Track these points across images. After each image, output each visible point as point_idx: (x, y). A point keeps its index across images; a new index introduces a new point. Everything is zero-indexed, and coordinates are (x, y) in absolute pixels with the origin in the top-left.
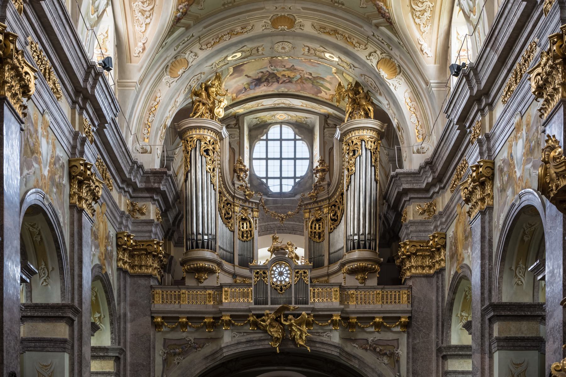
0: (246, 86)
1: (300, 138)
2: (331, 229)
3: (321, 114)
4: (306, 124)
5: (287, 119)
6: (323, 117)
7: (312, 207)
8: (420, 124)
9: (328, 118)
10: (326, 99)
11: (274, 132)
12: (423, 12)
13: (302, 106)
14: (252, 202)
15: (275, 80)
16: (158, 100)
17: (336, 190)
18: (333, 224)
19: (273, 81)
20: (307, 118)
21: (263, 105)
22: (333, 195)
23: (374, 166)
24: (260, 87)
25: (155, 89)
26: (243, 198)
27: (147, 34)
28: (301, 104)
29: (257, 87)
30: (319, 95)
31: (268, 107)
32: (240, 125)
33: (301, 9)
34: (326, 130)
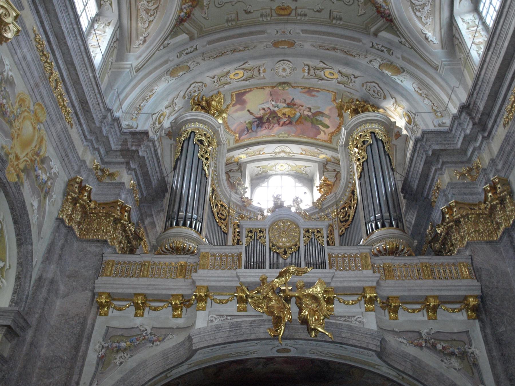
0: (249, 126)
4: (305, 173)
5: (287, 170)
6: (322, 164)
8: (435, 105)
10: (325, 141)
12: (423, 6)
14: (251, 211)
15: (276, 121)
16: (154, 91)
17: (345, 191)
20: (306, 167)
24: (262, 129)
27: (149, 30)
28: (300, 151)
29: (259, 129)
30: (318, 137)
31: (268, 156)
32: (242, 170)
33: (301, 33)
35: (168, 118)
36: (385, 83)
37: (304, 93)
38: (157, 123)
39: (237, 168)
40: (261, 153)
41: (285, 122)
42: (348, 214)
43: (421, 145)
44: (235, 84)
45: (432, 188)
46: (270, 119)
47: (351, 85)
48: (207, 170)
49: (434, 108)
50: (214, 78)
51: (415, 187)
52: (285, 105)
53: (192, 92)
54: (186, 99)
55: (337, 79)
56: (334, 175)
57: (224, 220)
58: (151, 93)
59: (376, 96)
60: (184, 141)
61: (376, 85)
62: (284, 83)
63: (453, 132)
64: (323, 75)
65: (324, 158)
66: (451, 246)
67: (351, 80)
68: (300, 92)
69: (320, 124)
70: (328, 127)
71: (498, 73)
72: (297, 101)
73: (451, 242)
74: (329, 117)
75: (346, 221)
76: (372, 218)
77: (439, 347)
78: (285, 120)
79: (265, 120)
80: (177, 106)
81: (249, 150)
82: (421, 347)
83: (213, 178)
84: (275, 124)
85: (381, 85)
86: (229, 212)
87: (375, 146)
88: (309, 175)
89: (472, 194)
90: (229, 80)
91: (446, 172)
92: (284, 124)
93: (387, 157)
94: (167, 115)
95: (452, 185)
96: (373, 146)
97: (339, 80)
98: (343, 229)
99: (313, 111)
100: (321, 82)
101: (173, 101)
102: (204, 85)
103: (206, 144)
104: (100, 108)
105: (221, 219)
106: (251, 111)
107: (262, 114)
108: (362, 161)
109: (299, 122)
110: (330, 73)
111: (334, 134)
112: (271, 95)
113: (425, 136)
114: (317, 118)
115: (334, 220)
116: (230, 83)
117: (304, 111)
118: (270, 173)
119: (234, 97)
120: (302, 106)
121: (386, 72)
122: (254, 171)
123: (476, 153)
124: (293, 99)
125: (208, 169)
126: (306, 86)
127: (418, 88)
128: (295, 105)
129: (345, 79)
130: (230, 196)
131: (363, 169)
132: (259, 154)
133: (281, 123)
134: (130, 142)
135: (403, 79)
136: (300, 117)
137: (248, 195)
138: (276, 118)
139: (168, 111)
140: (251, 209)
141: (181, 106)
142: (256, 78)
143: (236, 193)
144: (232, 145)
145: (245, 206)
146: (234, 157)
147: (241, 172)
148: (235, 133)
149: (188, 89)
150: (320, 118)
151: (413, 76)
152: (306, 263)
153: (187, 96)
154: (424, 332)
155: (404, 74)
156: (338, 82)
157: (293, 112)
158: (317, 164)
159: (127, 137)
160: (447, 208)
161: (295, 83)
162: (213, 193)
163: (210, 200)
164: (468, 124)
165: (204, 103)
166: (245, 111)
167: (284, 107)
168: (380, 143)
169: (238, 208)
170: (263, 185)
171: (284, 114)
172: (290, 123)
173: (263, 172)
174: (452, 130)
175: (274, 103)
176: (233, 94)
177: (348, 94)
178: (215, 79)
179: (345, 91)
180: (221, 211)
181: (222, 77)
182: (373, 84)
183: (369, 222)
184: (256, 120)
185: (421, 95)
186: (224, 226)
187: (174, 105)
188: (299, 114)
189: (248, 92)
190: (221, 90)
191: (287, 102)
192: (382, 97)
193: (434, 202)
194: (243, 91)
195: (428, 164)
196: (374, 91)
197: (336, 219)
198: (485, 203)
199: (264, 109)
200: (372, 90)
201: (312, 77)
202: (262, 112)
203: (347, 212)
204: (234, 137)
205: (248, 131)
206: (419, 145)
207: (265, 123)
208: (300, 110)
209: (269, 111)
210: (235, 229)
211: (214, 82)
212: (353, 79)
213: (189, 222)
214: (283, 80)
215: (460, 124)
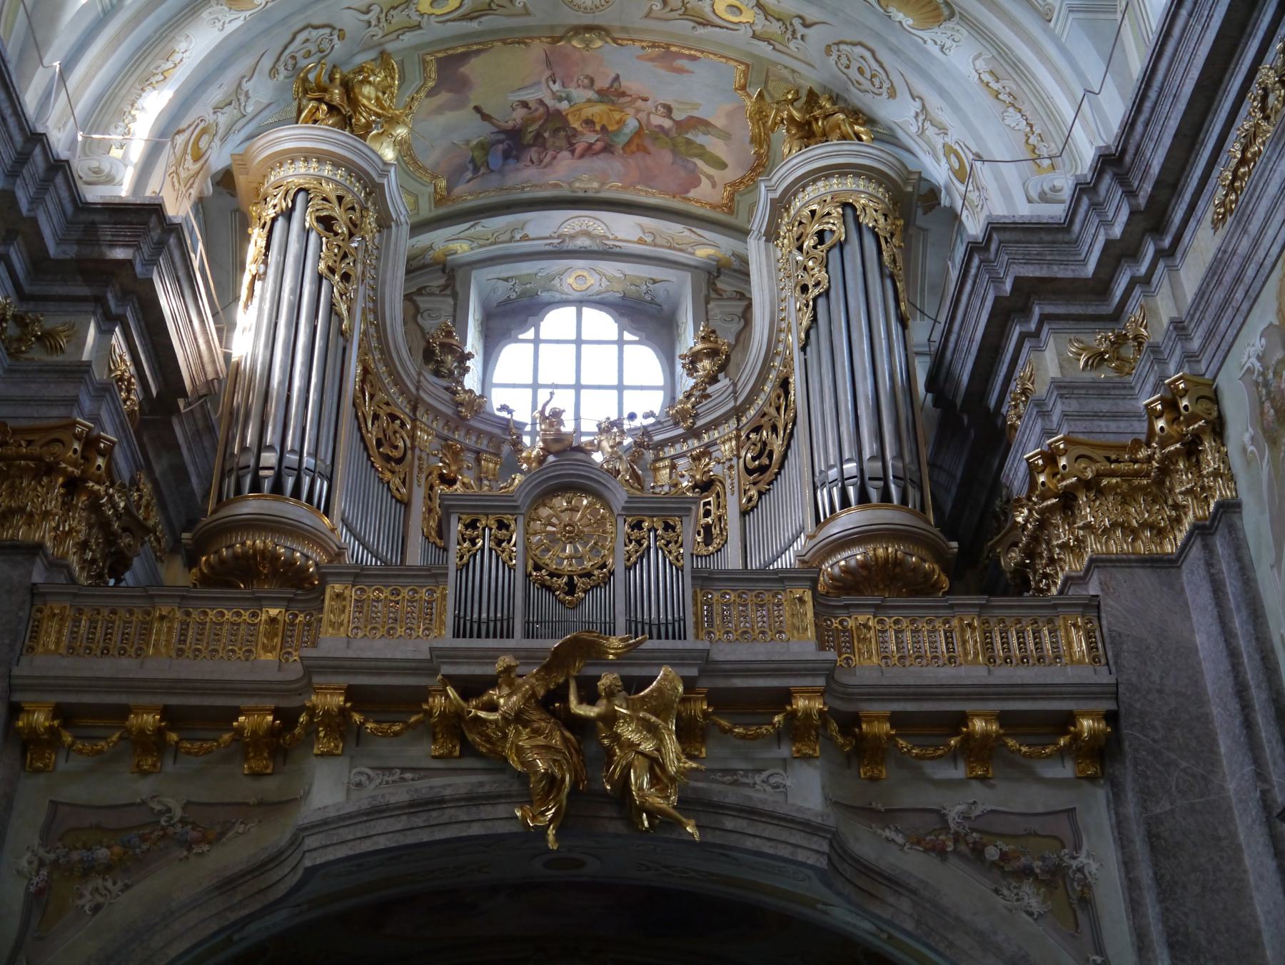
0: (477, 154)
1: (637, 338)
2: (750, 500)
3: (696, 267)
5: (596, 288)
6: (704, 276)
7: (678, 451)
8: (1037, 130)
9: (718, 277)
10: (713, 207)
11: (558, 322)
13: (641, 241)
14: (480, 433)
15: (564, 143)
16: (177, 58)
17: (762, 378)
18: (755, 484)
19: (558, 144)
20: (655, 282)
21: (525, 238)
22: (750, 400)
23: (892, 277)
24: (521, 165)
25: (172, 35)
26: (449, 412)
30: (692, 194)
31: (539, 245)
32: (458, 288)
34: (711, 305)
35: (223, 140)
36: (895, 51)
37: (652, 60)
38: (189, 157)
39: (442, 282)
40: (518, 237)
41: (590, 146)
42: (768, 448)
43: (981, 261)
44: (434, 31)
45: (1012, 387)
46: (546, 135)
47: (792, 45)
48: (345, 313)
49: (1033, 140)
50: (367, 12)
51: (965, 379)
52: (591, 94)
53: (299, 55)
54: (281, 77)
55: (751, 25)
56: (739, 311)
57: (399, 461)
58: (170, 65)
59: (866, 84)
60: (274, 220)
61: (868, 55)
62: (589, 28)
63: (1076, 227)
64: (708, 9)
65: (709, 257)
66: (1047, 565)
67: (794, 32)
68: (639, 58)
69: (700, 156)
70: (723, 166)
71: (1201, 74)
72: (626, 84)
73: (1050, 551)
74: (726, 136)
75: (762, 469)
76: (833, 473)
77: (992, 853)
78: (592, 138)
79: (529, 138)
80: (251, 102)
81: (479, 228)
82: (942, 853)
83: (365, 333)
84: (561, 149)
85: (884, 55)
86: (413, 437)
87: (852, 250)
88: (665, 307)
89: (1115, 416)
90: (416, 18)
91: (1051, 342)
92: (589, 150)
93: (888, 283)
94: (221, 131)
95: (1063, 388)
96: (847, 249)
97: (758, 28)
98: (753, 492)
99: (678, 116)
100: (701, 31)
101: (239, 85)
102: (336, 33)
103: (342, 229)
104: (8, 131)
105: (388, 458)
106: (486, 111)
107: (519, 121)
108: (813, 292)
109: (634, 147)
110: (731, 6)
111: (742, 187)
112: (549, 63)
113: (995, 236)
114: (689, 136)
115: (728, 464)
116: (419, 27)
117: (649, 114)
118: (545, 296)
119: (433, 68)
120: (645, 100)
121: (900, 16)
122: (494, 290)
123: (1137, 291)
124: (617, 78)
125: (349, 310)
126: (656, 39)
127: (991, 73)
128: (623, 94)
129: (775, 27)
130: (417, 389)
131: (815, 319)
132: (511, 239)
133: (580, 148)
134: (106, 232)
135: (949, 43)
136: (639, 132)
137: (471, 381)
138: (562, 134)
139: (223, 119)
140: (482, 426)
141: (265, 101)
142: (501, 11)
143: (437, 373)
144: (427, 210)
145: (464, 419)
146: (431, 248)
147: (455, 296)
148: (436, 177)
149: (286, 48)
150: (700, 139)
151: (979, 31)
152: (629, 621)
153: (282, 69)
154: (953, 813)
155: (950, 24)
156: (754, 36)
157: (617, 116)
158: (688, 277)
159: (97, 218)
160: (1043, 454)
161: (624, 29)
162: (363, 381)
163: (354, 405)
164: (1118, 208)
165: (336, 94)
166: (467, 114)
167: (589, 101)
168: (869, 240)
169: (441, 423)
170: (521, 337)
171: (589, 122)
172: (608, 149)
173: (523, 294)
174: (1072, 222)
175: (556, 87)
176: (429, 58)
177: (786, 73)
178: (372, 16)
179: (776, 64)
180: (390, 433)
181: (394, 8)
182: (859, 50)
183: (823, 485)
184: (502, 137)
185: (997, 95)
186: (397, 481)
187: (242, 98)
188: (636, 124)
189: (478, 52)
190: (390, 47)
191: (598, 85)
192: (884, 90)
193: (1014, 427)
194: (460, 50)
195: (1004, 314)
196: (860, 70)
197: (734, 462)
198: (1148, 445)
199: (525, 104)
200: (854, 66)
201: (675, 14)
202: (520, 113)
203: (765, 444)
204: (431, 189)
205: (476, 169)
206: (976, 261)
207: (530, 146)
208: (638, 111)
209: (541, 110)
210: (431, 488)
211: (369, 24)
212: (801, 30)
213: (290, 482)
214: (587, 20)
215: (1096, 206)
